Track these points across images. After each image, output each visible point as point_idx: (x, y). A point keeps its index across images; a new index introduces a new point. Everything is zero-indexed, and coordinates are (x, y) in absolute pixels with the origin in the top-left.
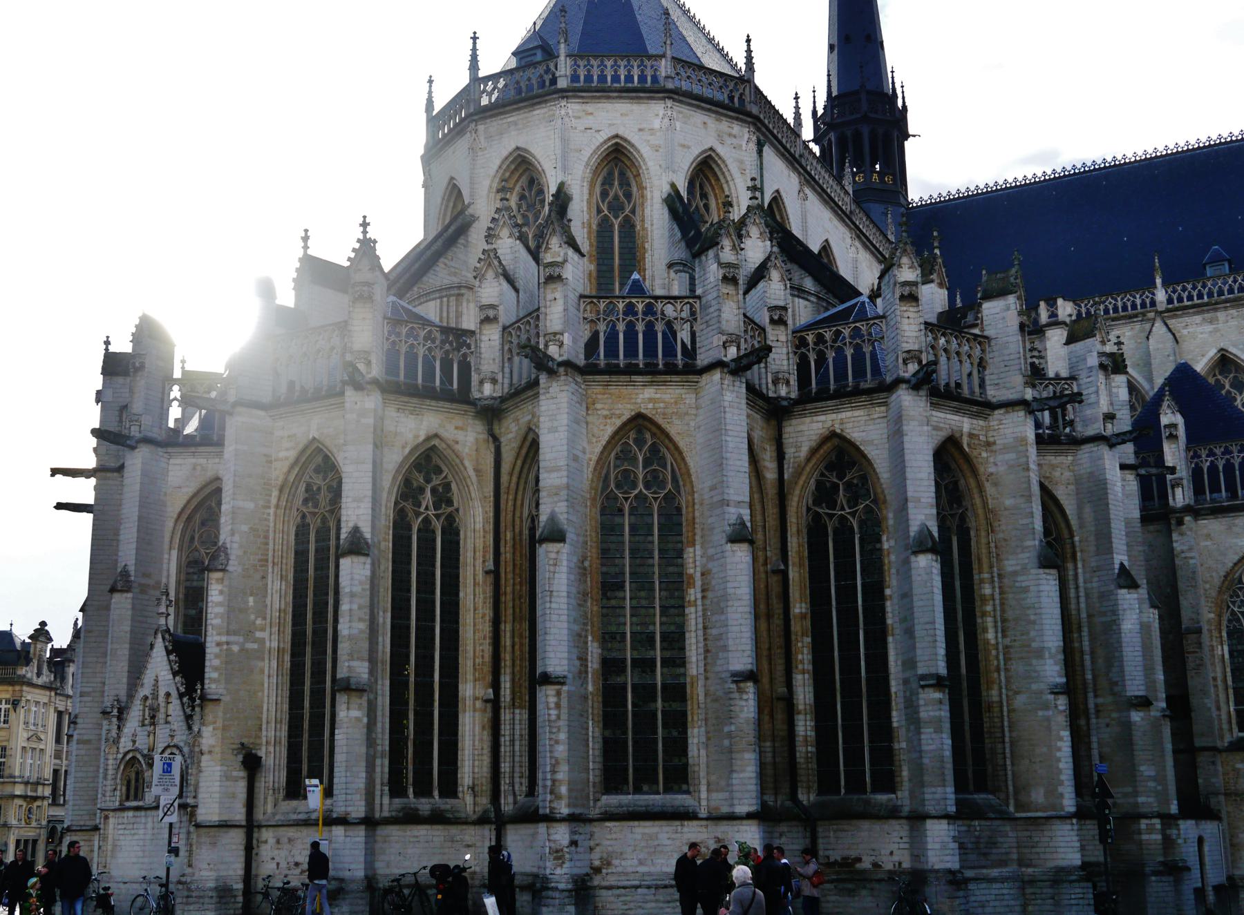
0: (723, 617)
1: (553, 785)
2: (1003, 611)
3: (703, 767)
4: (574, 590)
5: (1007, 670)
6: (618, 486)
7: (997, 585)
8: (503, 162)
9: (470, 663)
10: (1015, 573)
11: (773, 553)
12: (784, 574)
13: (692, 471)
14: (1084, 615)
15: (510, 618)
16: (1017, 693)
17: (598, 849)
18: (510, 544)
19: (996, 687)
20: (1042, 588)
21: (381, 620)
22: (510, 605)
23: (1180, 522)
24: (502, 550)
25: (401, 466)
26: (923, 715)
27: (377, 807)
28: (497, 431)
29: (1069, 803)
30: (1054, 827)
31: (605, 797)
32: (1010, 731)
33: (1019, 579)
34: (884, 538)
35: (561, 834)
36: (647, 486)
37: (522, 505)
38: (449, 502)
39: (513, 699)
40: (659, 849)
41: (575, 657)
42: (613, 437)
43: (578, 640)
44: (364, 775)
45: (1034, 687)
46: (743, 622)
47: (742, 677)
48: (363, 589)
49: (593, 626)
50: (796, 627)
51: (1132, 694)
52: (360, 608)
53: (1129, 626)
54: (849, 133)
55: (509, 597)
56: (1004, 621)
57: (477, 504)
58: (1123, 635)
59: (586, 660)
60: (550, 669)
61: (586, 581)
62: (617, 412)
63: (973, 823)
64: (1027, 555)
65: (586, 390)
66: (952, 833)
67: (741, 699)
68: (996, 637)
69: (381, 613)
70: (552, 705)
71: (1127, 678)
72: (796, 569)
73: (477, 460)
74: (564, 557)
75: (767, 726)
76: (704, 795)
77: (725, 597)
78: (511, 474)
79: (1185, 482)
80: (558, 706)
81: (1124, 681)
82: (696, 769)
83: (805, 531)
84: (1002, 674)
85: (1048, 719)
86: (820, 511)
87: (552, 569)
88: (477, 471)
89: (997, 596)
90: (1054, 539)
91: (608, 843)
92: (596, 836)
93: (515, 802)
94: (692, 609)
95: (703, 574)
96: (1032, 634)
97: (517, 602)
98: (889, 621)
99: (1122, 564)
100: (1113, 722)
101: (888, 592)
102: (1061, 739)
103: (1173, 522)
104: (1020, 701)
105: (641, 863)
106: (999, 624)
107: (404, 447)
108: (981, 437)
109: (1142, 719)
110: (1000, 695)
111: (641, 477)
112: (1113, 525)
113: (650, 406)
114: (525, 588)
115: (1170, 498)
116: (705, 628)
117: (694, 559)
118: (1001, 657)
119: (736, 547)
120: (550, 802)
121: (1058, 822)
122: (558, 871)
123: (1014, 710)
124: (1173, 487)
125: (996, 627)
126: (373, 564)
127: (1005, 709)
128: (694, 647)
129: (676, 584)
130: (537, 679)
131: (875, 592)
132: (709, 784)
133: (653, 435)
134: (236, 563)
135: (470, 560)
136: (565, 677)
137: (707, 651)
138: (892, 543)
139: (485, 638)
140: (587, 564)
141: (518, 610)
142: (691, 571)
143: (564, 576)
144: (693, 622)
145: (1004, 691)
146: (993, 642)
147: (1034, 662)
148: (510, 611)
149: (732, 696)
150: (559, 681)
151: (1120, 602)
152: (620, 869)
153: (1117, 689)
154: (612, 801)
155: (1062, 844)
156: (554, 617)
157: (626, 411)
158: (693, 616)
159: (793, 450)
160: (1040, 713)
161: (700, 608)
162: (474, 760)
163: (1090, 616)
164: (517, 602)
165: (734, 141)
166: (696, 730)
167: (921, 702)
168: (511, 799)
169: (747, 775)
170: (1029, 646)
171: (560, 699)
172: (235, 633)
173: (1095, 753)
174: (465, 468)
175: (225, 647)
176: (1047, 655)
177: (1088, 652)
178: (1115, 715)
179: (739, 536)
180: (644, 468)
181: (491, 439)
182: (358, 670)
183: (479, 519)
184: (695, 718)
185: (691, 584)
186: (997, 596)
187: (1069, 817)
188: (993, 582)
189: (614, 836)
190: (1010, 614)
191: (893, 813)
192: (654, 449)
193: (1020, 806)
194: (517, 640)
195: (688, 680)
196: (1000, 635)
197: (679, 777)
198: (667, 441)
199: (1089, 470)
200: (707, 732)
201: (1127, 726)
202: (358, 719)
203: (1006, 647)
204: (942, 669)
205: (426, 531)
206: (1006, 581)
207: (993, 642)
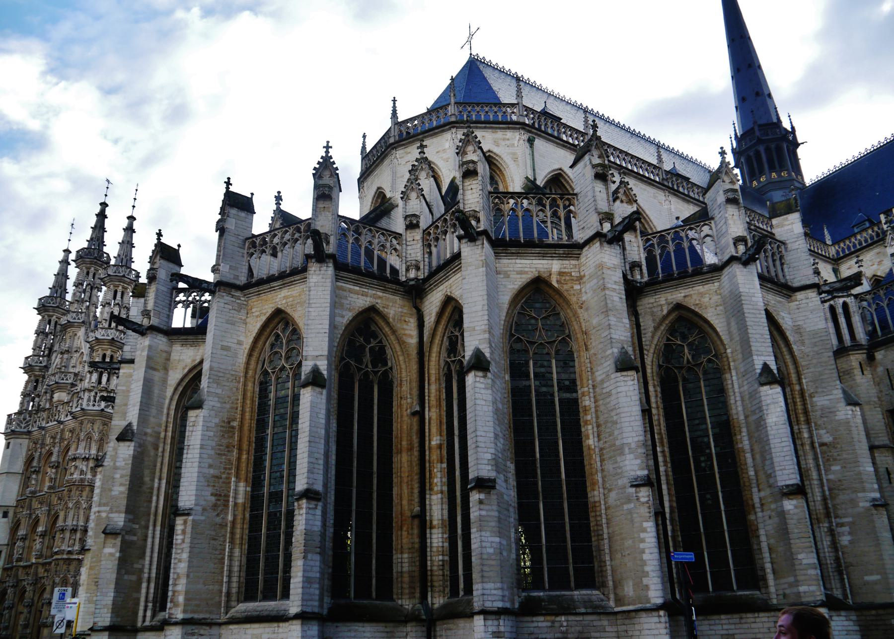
1: (173, 595)
8: (373, 199)
10: (602, 382)
16: (610, 490)
20: (619, 390)
27: (140, 619)
29: (656, 595)
30: (642, 620)
32: (608, 528)
33: (605, 385)
44: (112, 594)
45: (620, 482)
48: (126, 464)
51: (783, 483)
52: (121, 477)
53: (774, 419)
54: (752, 154)
58: (769, 428)
62: (264, 311)
63: (558, 619)
64: (609, 363)
65: (247, 301)
70: (179, 532)
71: (777, 469)
74: (201, 419)
80: (184, 532)
81: (774, 471)
96: (616, 432)
102: (644, 530)
107: (184, 369)
108: (573, 274)
112: (750, 331)
113: (284, 301)
120: (170, 608)
121: (644, 614)
134: (110, 460)
140: (235, 424)
143: (200, 433)
147: (619, 459)
150: (187, 513)
151: (763, 398)
156: (189, 465)
157: (269, 310)
160: (626, 507)
163: (746, 417)
165: (507, 142)
170: (615, 445)
171: (185, 527)
172: (105, 505)
173: (764, 545)
175: (97, 514)
176: (627, 450)
177: (749, 451)
178: (773, 506)
182: (116, 519)
190: (601, 420)
193: (619, 601)
199: (729, 289)
201: (782, 515)
202: (111, 554)
206: (597, 390)
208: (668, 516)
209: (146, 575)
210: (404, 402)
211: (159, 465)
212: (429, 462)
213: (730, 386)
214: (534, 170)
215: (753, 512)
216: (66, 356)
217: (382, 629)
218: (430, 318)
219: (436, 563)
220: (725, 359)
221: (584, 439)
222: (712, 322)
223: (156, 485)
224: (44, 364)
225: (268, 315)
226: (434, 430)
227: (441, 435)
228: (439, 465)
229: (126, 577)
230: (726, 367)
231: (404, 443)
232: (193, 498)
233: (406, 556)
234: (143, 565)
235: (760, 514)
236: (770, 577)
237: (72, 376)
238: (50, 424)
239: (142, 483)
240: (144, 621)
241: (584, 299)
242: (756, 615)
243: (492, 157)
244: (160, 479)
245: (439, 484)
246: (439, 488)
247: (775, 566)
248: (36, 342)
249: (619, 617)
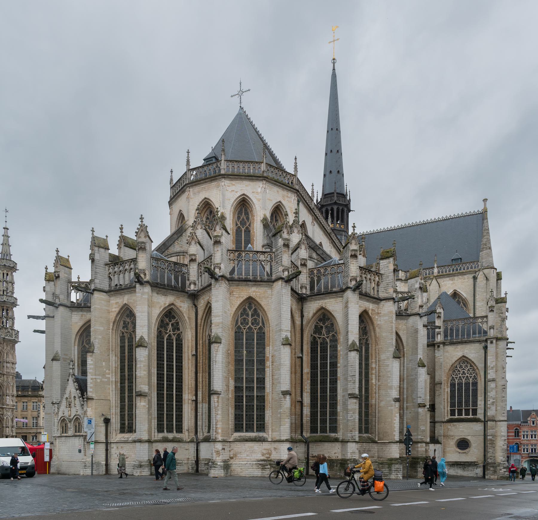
0: (279, 372)
2: (379, 373)
3: (270, 424)
4: (224, 361)
5: (378, 393)
6: (241, 324)
7: (377, 363)
9: (187, 387)
11: (298, 350)
12: (301, 358)
13: (269, 319)
14: (405, 376)
15: (201, 371)
17: (232, 451)
18: (201, 345)
19: (374, 399)
21: (153, 371)
22: (201, 367)
23: (439, 347)
24: (198, 347)
25: (159, 315)
26: (349, 407)
28: (196, 303)
31: (235, 434)
34: (339, 346)
35: (219, 446)
36: (252, 324)
37: (206, 331)
38: (178, 329)
39: (202, 400)
40: (254, 451)
41: (224, 385)
42: (240, 305)
43: (227, 379)
45: (388, 399)
46: (287, 373)
47: (285, 393)
49: (231, 374)
50: (305, 377)
55: (201, 364)
56: (379, 377)
57: (189, 330)
59: (229, 386)
60: (215, 389)
61: (229, 358)
66: (357, 447)
67: (285, 400)
68: (376, 382)
69: (153, 369)
72: (306, 357)
73: (189, 314)
75: (293, 410)
76: (270, 433)
77: (280, 364)
78: (202, 320)
79: (442, 333)
82: (268, 424)
83: (310, 343)
84: (377, 394)
85: (392, 410)
86: (315, 335)
87: (216, 353)
88: (189, 318)
89: (377, 368)
91: (236, 449)
92: (232, 447)
93: (203, 435)
94: (268, 369)
95: (272, 357)
96: (389, 381)
97: (204, 366)
98: (338, 375)
99: (420, 358)
101: (339, 365)
102: (396, 417)
103: (436, 346)
104: (382, 404)
105: (247, 456)
106: (377, 377)
109: (423, 411)
110: (376, 402)
111: (250, 321)
114: (207, 361)
115: (436, 338)
116: (272, 376)
117: (269, 351)
118: (377, 389)
119: (285, 346)
121: (392, 444)
122: (218, 458)
123: (380, 407)
124: (437, 334)
125: (376, 378)
126: (149, 350)
127: (377, 406)
128: (268, 382)
129: (262, 362)
131: (334, 365)
132: (272, 430)
133: (255, 305)
135: (186, 350)
136: (221, 392)
137: (273, 384)
138: (342, 348)
139: (192, 379)
141: (204, 369)
142: (268, 355)
144: (268, 374)
145: (377, 400)
146: (374, 383)
147: (389, 390)
148: (201, 369)
149: (282, 399)
152: (240, 458)
154: (237, 435)
158: (268, 371)
159: (307, 313)
160: (389, 408)
161: (271, 369)
162: (188, 421)
163: (407, 376)
164: (204, 366)
166: (268, 411)
167: (349, 403)
168: (201, 434)
169: (286, 427)
170: (387, 385)
174: (184, 317)
179: (287, 343)
180: (251, 317)
181: (194, 306)
183: (190, 336)
184: (268, 407)
185: (268, 360)
186: (377, 368)
187: (397, 442)
188: (376, 363)
189: (238, 447)
190: (381, 374)
191: (336, 440)
192: (255, 310)
194: (204, 379)
195: (266, 394)
196: (377, 381)
197: (262, 427)
198: (260, 308)
200: (272, 412)
201: (418, 413)
203: (379, 385)
204: (357, 392)
205: (170, 338)
207: (374, 383)
221: (370, 380)
225: (244, 298)
232: (221, 387)
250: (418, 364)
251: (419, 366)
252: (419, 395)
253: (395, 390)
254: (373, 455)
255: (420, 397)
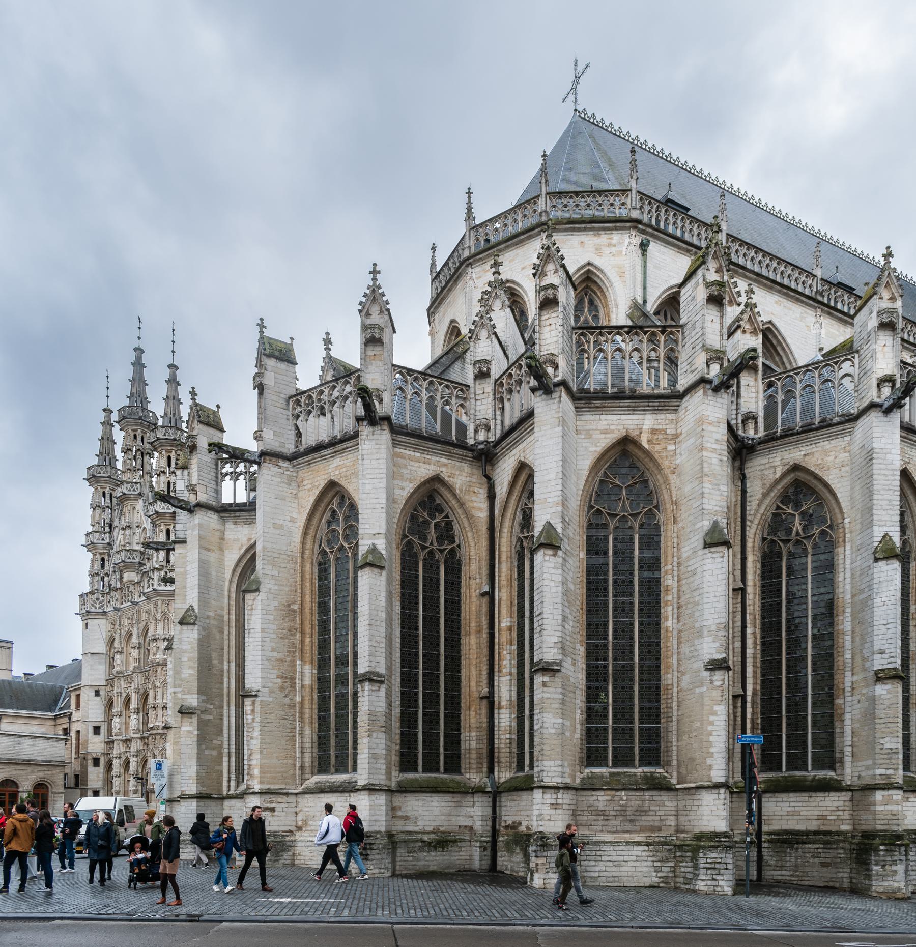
16: (684, 674)
29: (718, 774)
70: (249, 712)
80: (253, 712)
85: (702, 695)
90: (829, 527)
100: (863, 698)
109: (889, 692)
121: (704, 791)
130: (243, 694)
153: (868, 664)
155: (706, 812)
160: (697, 690)
177: (850, 633)
178: (864, 691)
208: (749, 698)
209: (226, 750)
210: (472, 582)
211: (226, 648)
212: (499, 644)
213: (841, 562)
214: (645, 288)
215: (842, 696)
216: (127, 532)
217: (449, 799)
218: (501, 490)
219: (503, 741)
220: (841, 530)
221: (662, 620)
222: (833, 487)
223: (226, 667)
224: (107, 541)
226: (504, 611)
227: (511, 617)
228: (509, 647)
229: (207, 752)
230: (841, 540)
231: (473, 625)
232: (260, 680)
233: (473, 734)
234: (222, 742)
235: (849, 699)
236: (848, 760)
237: (139, 554)
238: (125, 605)
239: (211, 666)
240: (229, 790)
241: (678, 462)
242: (827, 794)
243: (593, 273)
244: (229, 662)
245: (508, 666)
246: (508, 670)
247: (855, 749)
248: (93, 517)
249: (680, 793)
250: (874, 553)
251: (877, 560)
252: (878, 644)
253: (711, 639)
254: (657, 824)
255: (882, 652)
